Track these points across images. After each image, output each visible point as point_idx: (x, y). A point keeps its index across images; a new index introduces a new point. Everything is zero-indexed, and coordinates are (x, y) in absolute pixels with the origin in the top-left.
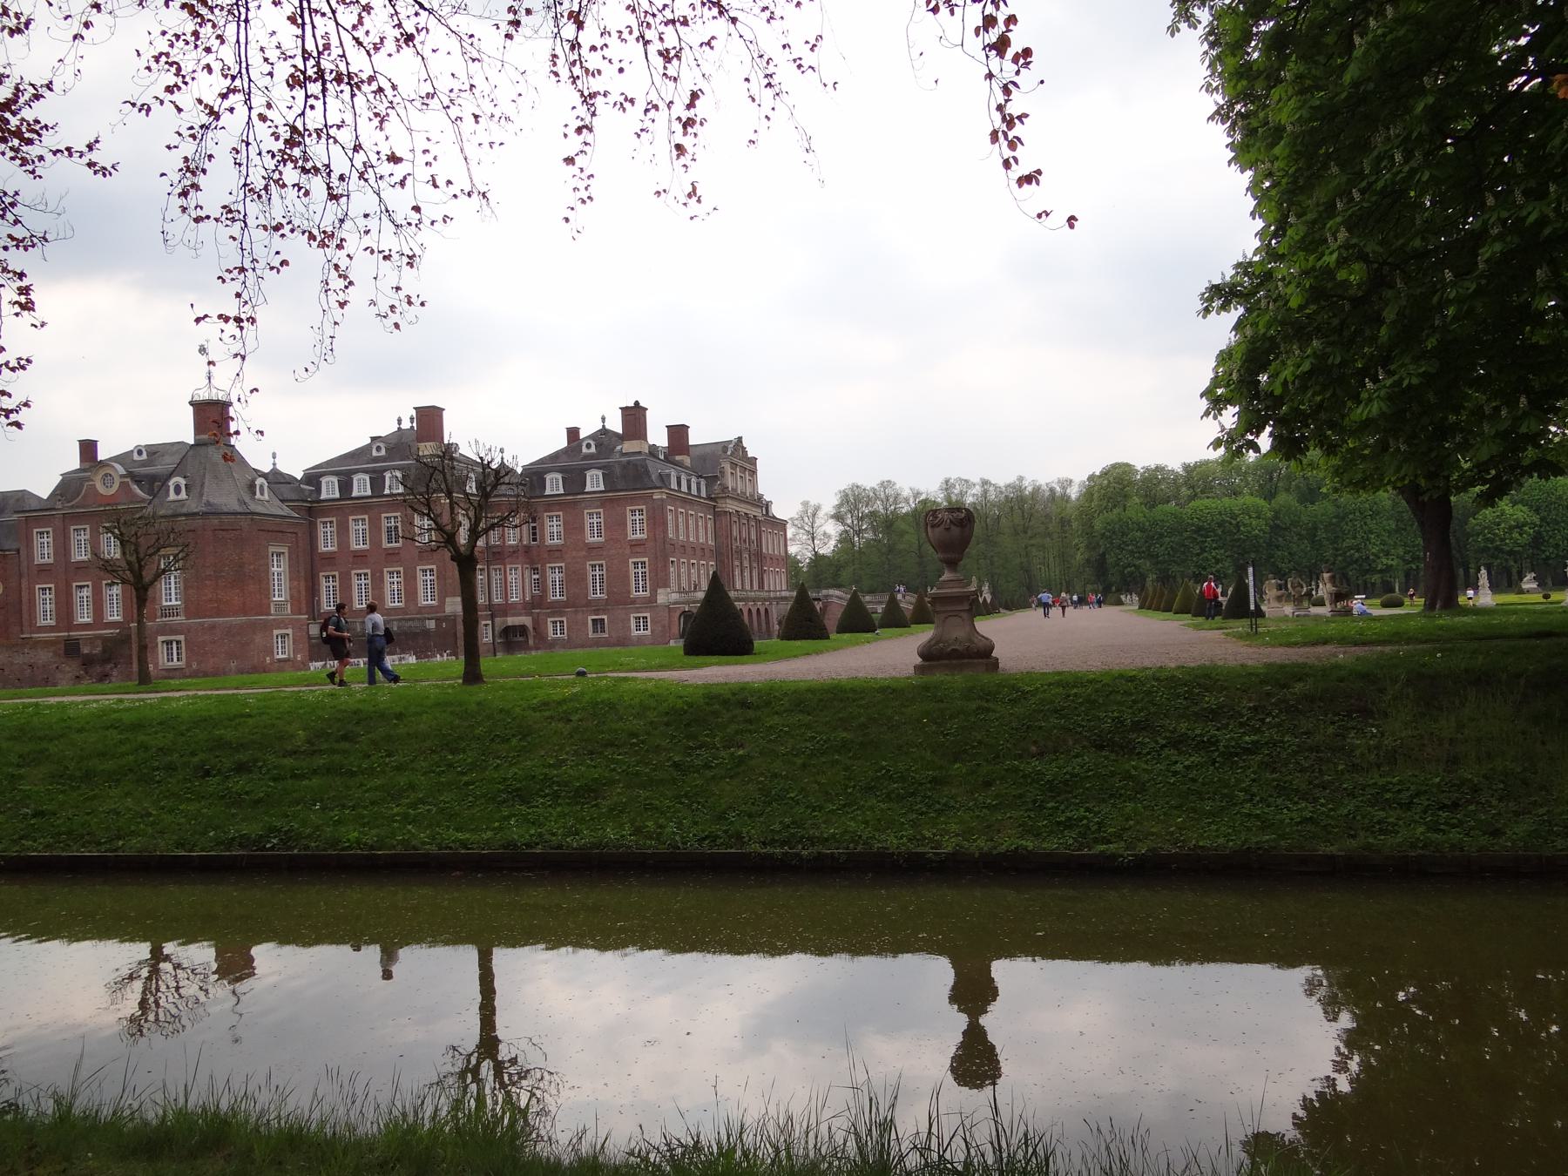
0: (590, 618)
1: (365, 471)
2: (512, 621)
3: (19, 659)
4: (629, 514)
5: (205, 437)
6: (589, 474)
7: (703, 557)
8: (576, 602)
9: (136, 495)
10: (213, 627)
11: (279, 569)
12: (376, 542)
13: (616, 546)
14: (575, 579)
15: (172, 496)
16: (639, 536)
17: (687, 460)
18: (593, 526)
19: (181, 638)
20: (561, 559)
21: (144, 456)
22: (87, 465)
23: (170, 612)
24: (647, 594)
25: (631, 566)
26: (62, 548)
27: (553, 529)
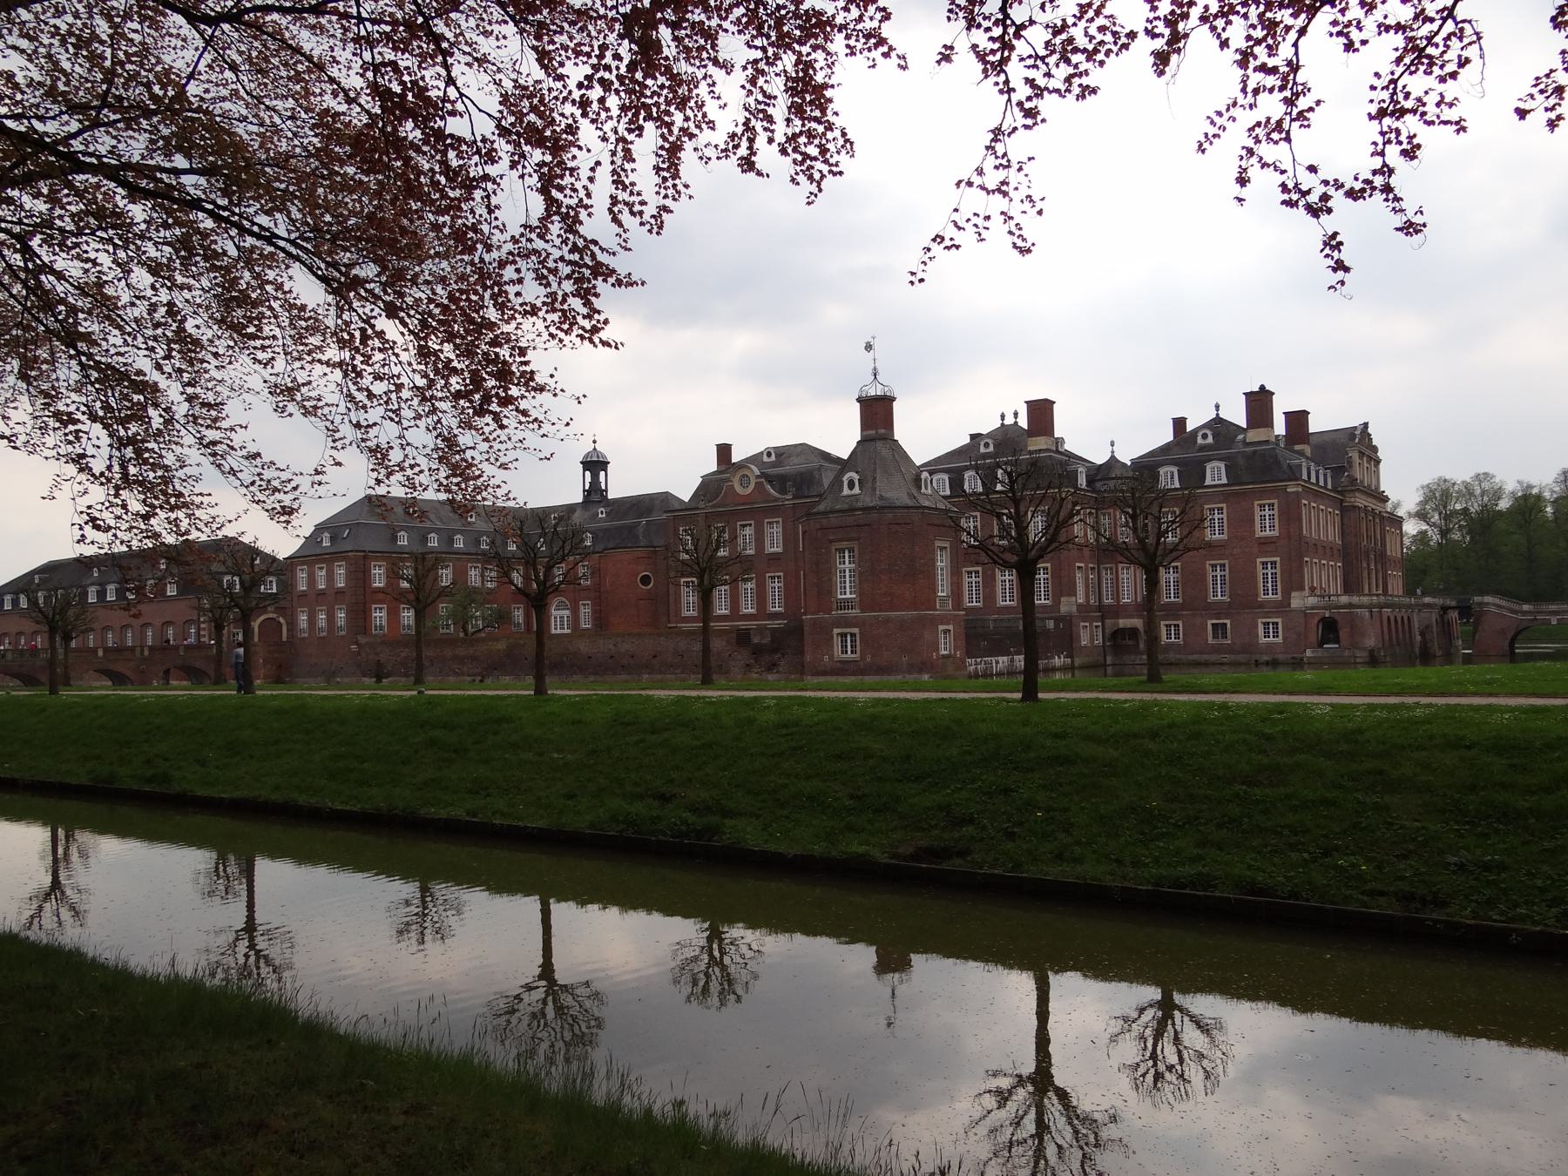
0: (1210, 622)
2: (1123, 623)
4: (1257, 509)
5: (872, 432)
6: (1209, 467)
7: (1332, 558)
8: (1194, 603)
10: (887, 620)
11: (942, 563)
13: (1242, 543)
15: (846, 491)
17: (1307, 449)
19: (856, 630)
21: (773, 458)
22: (723, 468)
23: (845, 604)
24: (1279, 597)
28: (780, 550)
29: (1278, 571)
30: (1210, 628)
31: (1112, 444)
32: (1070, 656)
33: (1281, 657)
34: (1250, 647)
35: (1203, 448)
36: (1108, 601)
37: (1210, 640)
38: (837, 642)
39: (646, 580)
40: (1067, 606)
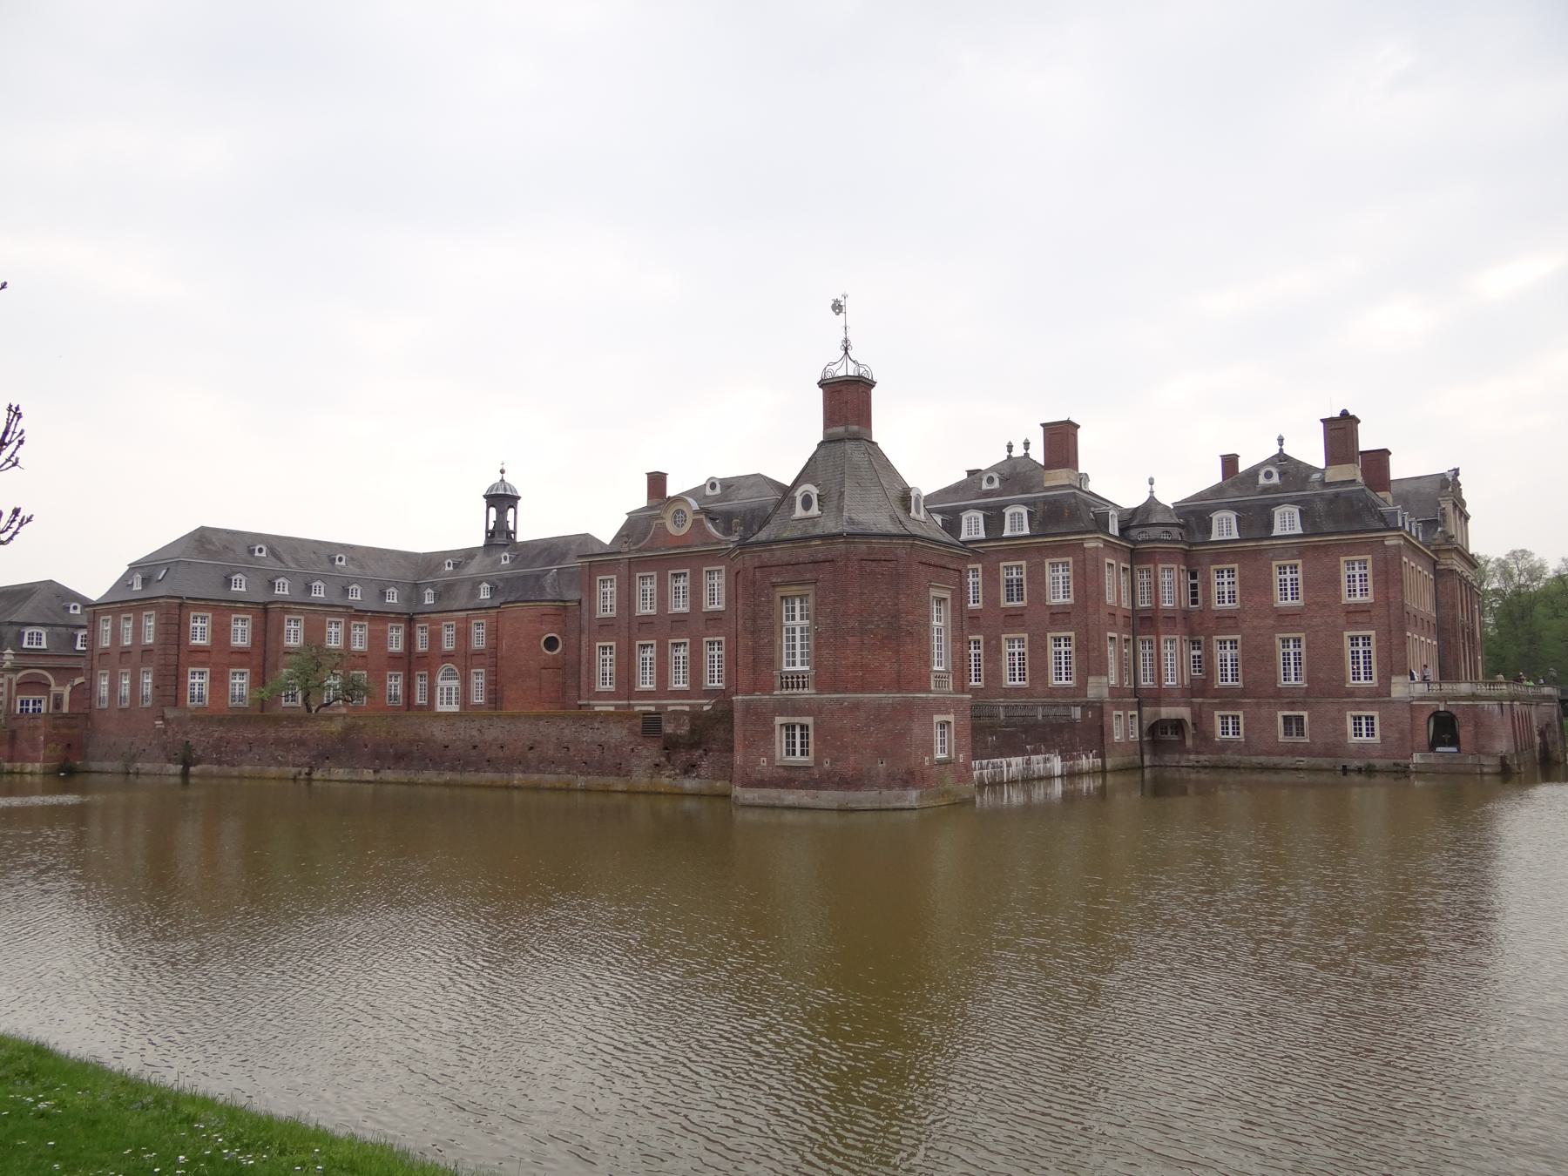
0: (1280, 714)
1: (976, 507)
2: (1167, 712)
3: (587, 736)
4: (1343, 567)
5: (840, 430)
6: (1278, 512)
8: (1259, 689)
9: (709, 535)
10: (856, 707)
11: (940, 622)
12: (991, 600)
14: (1257, 658)
15: (799, 512)
16: (1358, 598)
18: (1287, 586)
19: (809, 720)
20: (1235, 629)
21: (718, 491)
22: (655, 502)
24: (1374, 682)
25: (1347, 642)
26: (627, 599)
27: (1224, 589)
28: (721, 607)
29: (1373, 648)
30: (1280, 721)
31: (1151, 482)
32: (1101, 755)
33: (1379, 763)
34: (1334, 748)
35: (1266, 490)
36: (1146, 683)
37: (1281, 737)
38: (780, 737)
39: (551, 644)
40: (1097, 689)
